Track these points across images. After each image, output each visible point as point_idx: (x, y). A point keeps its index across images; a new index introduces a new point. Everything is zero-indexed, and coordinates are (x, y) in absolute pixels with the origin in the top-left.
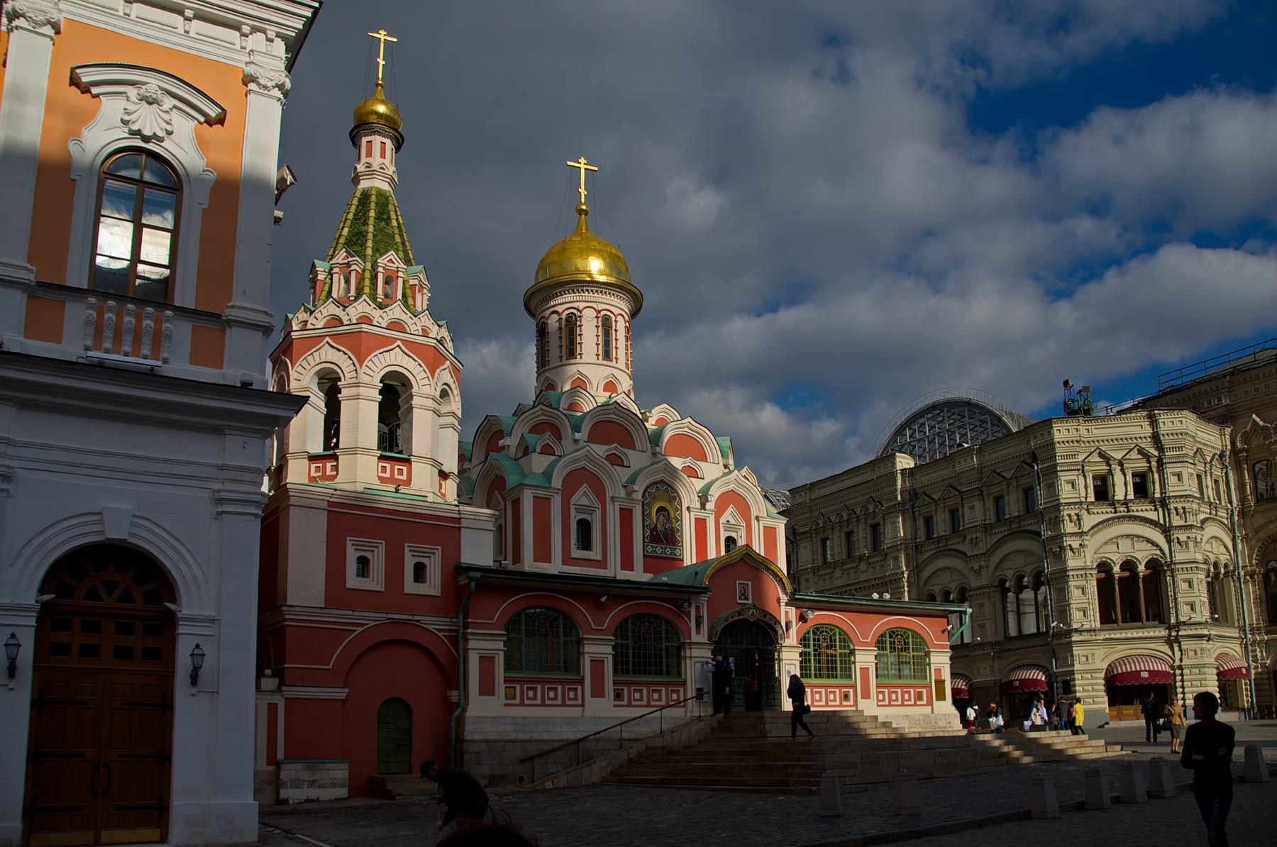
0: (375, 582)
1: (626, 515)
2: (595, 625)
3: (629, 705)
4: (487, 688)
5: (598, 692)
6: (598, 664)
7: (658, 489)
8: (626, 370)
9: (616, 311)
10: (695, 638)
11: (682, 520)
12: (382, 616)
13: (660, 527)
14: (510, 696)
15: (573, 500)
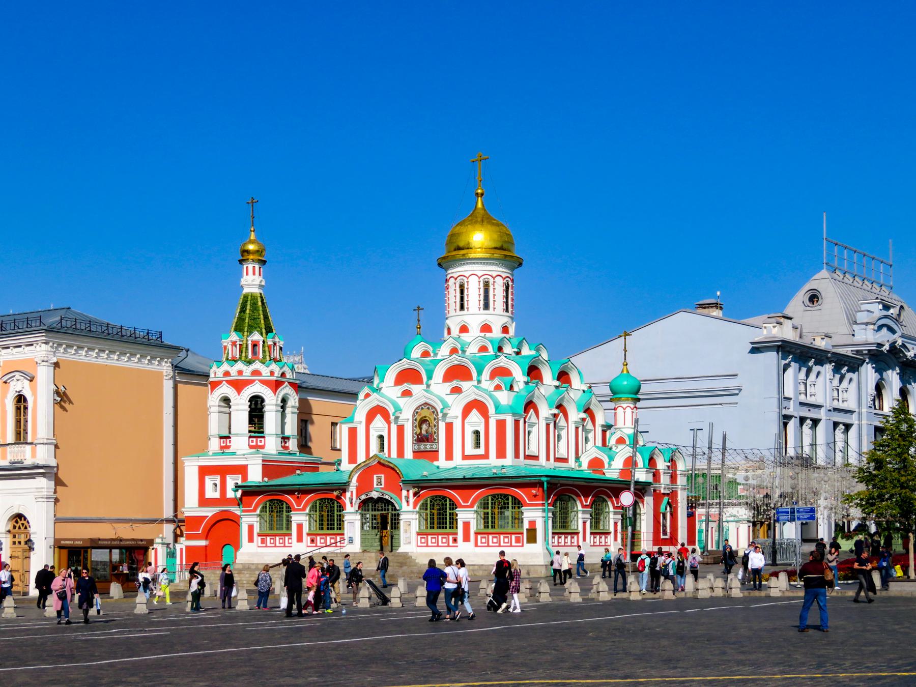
0: (217, 495)
1: (401, 429)
2: (297, 506)
3: (316, 546)
4: (251, 540)
5: (300, 539)
6: (300, 527)
7: (422, 408)
8: (482, 311)
9: (467, 274)
10: (349, 508)
11: (438, 426)
12: (217, 509)
13: (424, 432)
14: (263, 541)
15: (371, 426)
